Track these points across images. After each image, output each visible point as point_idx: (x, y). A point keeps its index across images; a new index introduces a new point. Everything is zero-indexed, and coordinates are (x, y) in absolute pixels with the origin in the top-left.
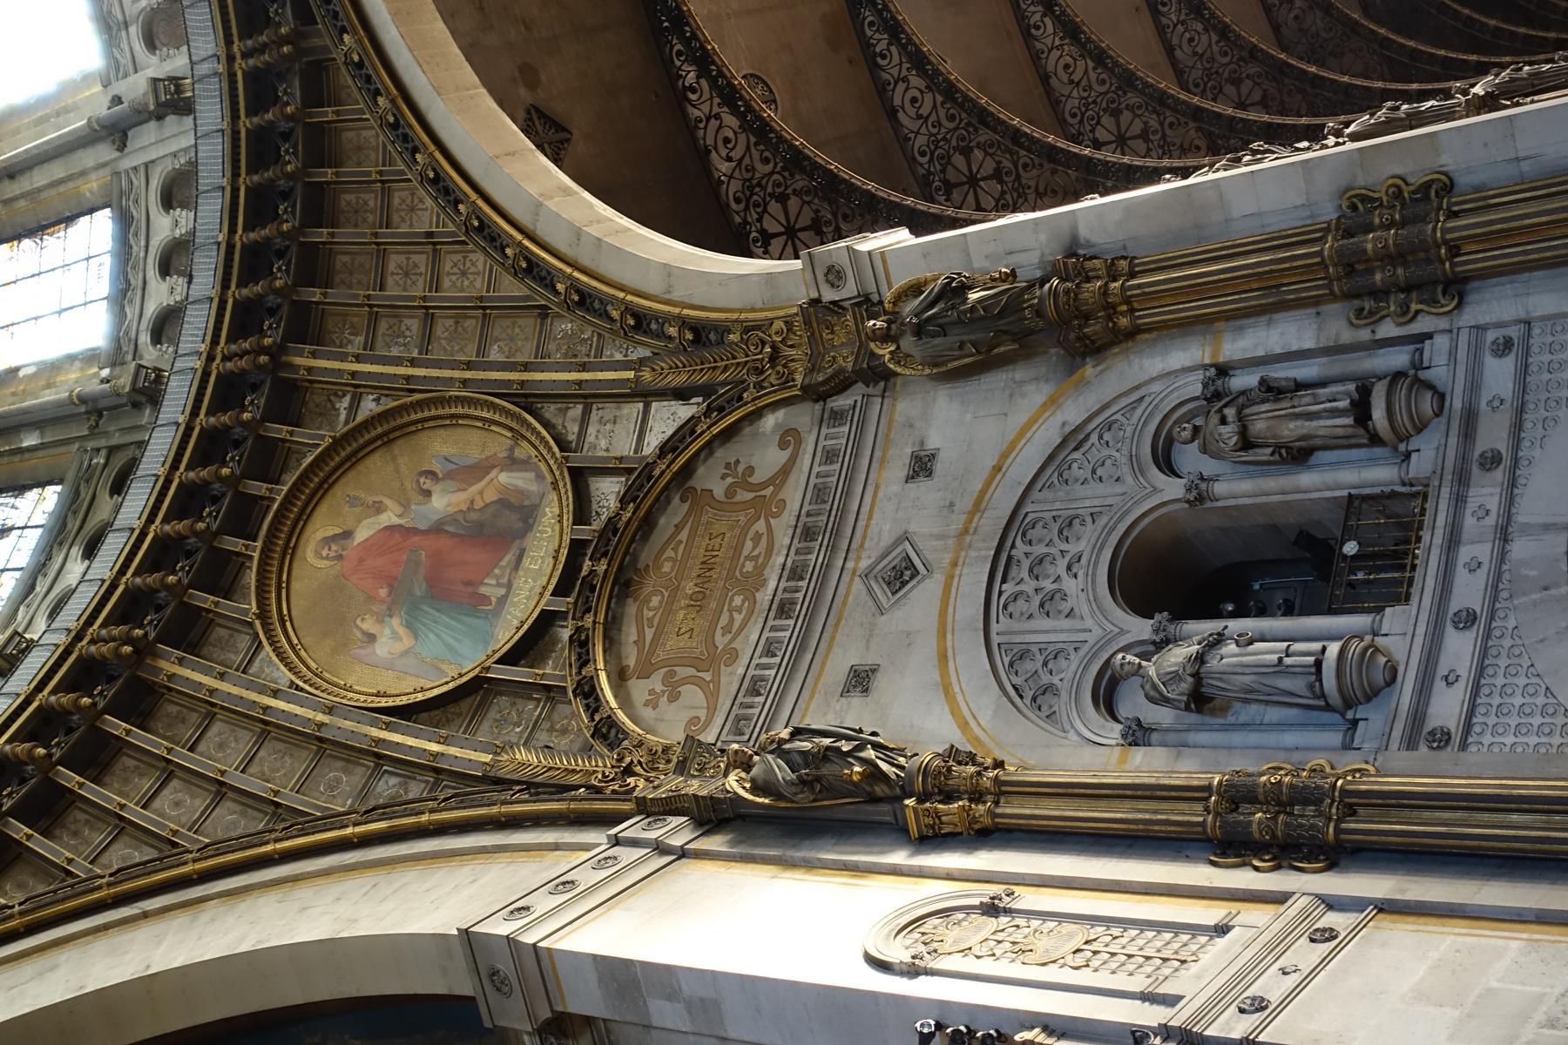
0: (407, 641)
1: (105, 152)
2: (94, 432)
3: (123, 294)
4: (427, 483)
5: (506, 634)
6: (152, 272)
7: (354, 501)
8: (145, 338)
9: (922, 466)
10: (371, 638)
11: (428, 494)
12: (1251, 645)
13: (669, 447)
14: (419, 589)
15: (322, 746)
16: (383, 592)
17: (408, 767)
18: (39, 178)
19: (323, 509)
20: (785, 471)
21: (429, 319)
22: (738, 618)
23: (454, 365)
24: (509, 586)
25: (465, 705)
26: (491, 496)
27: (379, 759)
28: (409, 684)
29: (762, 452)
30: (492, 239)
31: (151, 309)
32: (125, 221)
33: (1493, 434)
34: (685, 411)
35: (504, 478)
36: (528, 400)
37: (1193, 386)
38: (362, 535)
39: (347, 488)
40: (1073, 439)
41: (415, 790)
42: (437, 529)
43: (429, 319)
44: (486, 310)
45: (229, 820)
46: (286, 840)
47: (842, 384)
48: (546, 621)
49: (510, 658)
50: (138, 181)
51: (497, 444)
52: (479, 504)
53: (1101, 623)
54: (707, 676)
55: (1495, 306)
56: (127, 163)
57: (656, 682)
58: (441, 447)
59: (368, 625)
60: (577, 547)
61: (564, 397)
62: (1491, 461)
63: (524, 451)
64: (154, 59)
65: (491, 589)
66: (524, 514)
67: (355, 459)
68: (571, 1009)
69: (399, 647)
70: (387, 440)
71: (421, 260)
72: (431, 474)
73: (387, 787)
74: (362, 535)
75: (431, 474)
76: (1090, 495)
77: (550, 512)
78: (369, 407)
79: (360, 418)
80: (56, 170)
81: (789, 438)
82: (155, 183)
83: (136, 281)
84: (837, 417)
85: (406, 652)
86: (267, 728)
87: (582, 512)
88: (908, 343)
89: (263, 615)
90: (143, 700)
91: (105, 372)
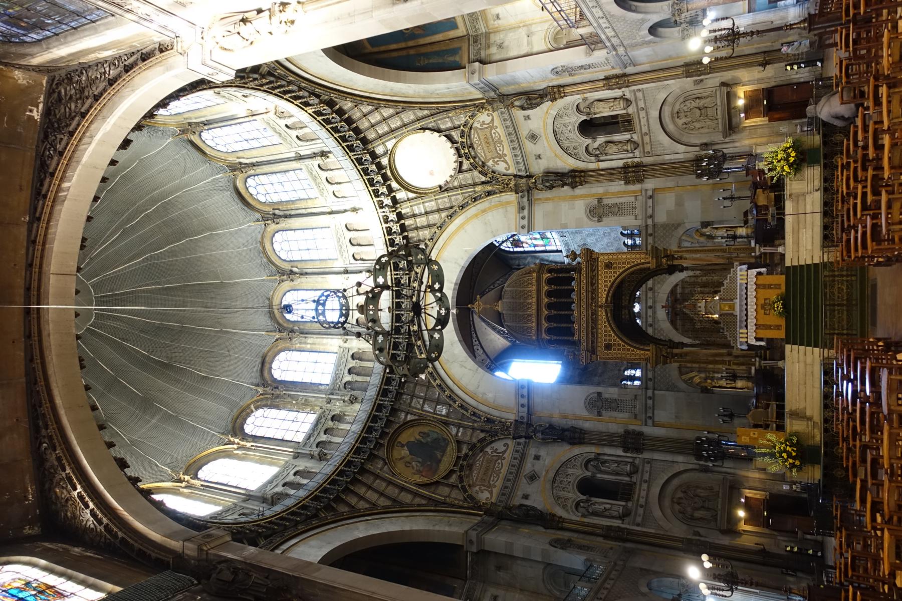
9: (537, 458)
12: (601, 504)
13: (480, 441)
15: (402, 489)
17: (422, 496)
20: (505, 451)
27: (416, 494)
29: (499, 446)
33: (646, 477)
34: (482, 435)
37: (593, 456)
40: (569, 460)
41: (424, 502)
45: (383, 502)
46: (397, 508)
47: (520, 437)
48: (452, 472)
53: (575, 495)
55: (647, 455)
57: (477, 488)
60: (458, 458)
62: (646, 481)
68: (486, 549)
71: (425, 389)
73: (418, 500)
76: (570, 471)
78: (409, 417)
81: (506, 445)
84: (519, 444)
86: (390, 483)
88: (539, 435)
90: (363, 471)
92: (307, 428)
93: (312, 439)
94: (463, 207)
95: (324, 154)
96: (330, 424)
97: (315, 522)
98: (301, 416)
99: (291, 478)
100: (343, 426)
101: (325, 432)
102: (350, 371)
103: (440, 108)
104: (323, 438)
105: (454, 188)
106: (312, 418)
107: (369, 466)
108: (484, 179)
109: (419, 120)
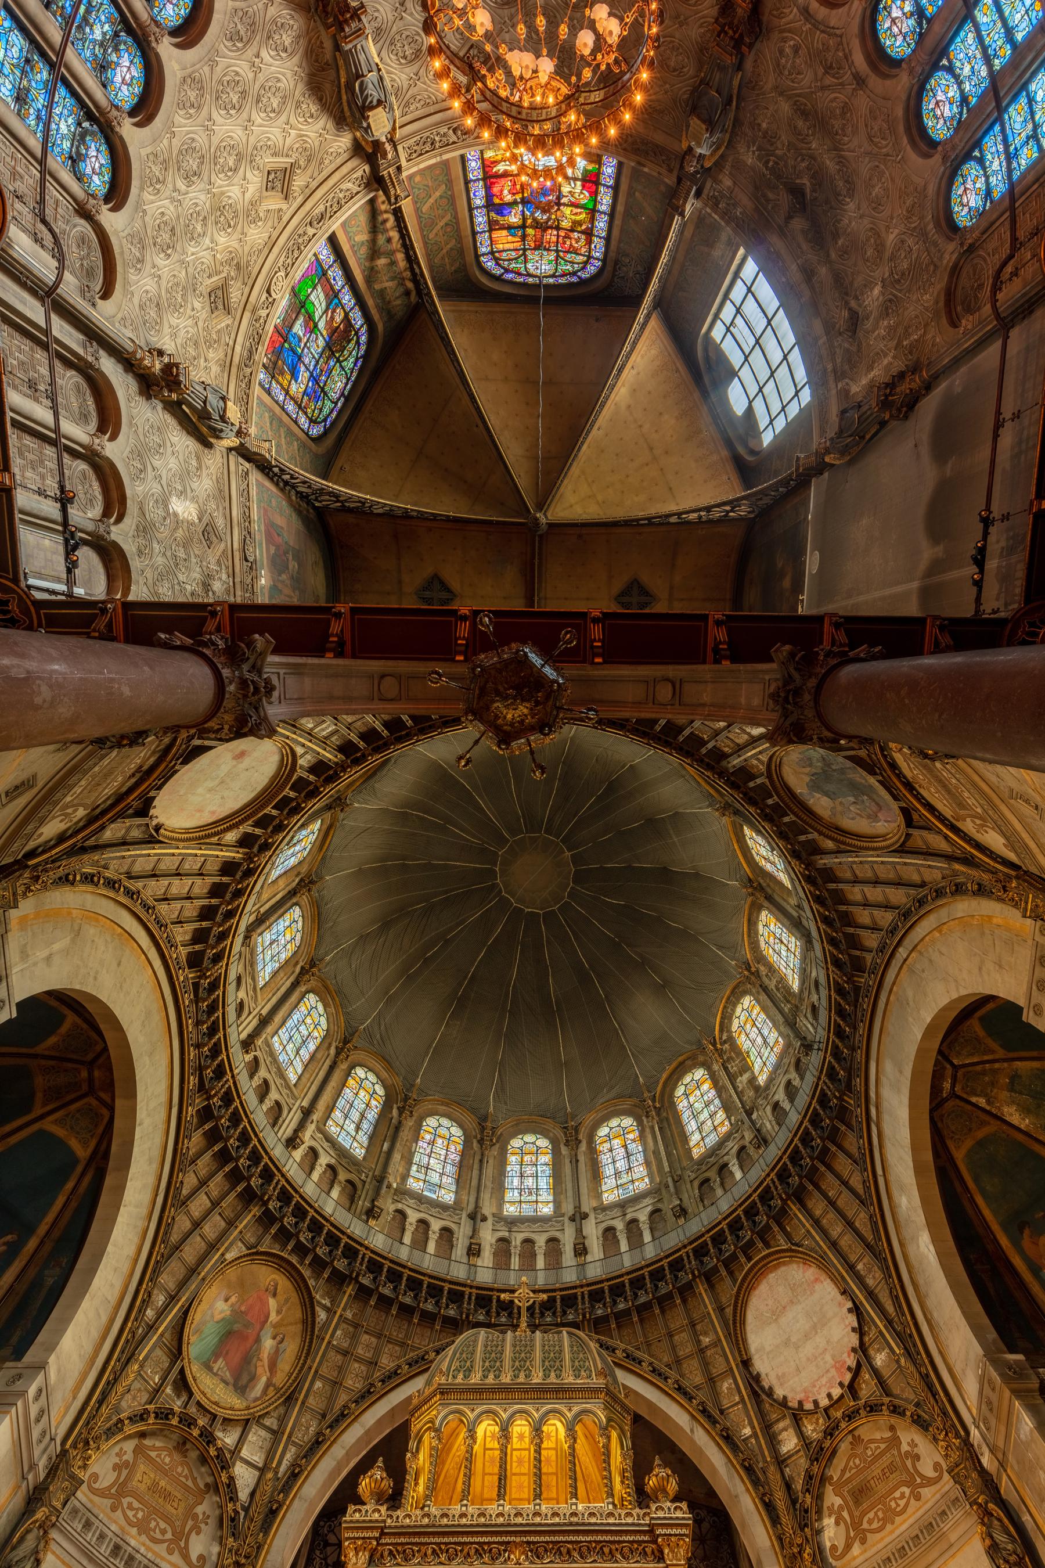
0: (218, 1317)
1: (471, 1207)
2: (374, 1176)
3: (420, 1199)
4: (278, 1338)
5: (195, 1371)
6: (422, 1215)
7: (287, 1301)
8: (400, 1206)
10: (226, 1300)
11: (274, 1338)
14: (237, 1327)
16: (243, 1308)
18: (475, 1172)
19: (290, 1286)
21: (345, 1353)
22: (130, 1514)
23: (320, 1364)
24: (216, 1374)
25: (175, 1343)
26: (260, 1370)
28: (198, 1317)
30: (363, 1397)
31: (409, 1212)
32: (444, 1207)
35: (264, 1379)
36: (289, 1400)
38: (272, 1303)
39: (295, 1298)
42: (258, 1340)
43: (345, 1353)
44: (336, 1384)
49: (182, 1371)
50: (456, 1219)
51: (280, 1379)
52: (259, 1364)
54: (113, 1491)
56: (464, 1215)
58: (291, 1348)
59: (233, 1299)
61: (282, 1420)
63: (271, 1392)
64: (494, 1241)
65: (219, 1364)
66: (241, 1389)
67: (303, 1304)
69: (216, 1313)
70: (304, 1322)
72: (281, 1342)
74: (272, 1303)
75: (281, 1342)
77: (237, 1402)
79: (317, 1308)
80: (474, 1182)
82: (453, 1226)
83: (422, 1207)
85: (212, 1316)
87: (227, 1421)
89: (257, 1253)
91: (395, 1185)
92: (345, 1141)
93: (326, 1145)
94: (728, 1438)
95: (762, 1140)
96: (342, 1176)
97: (193, 1081)
98: (364, 1139)
99: (274, 1095)
100: (335, 1193)
101: (330, 1166)
102: (423, 1223)
103: (912, 1343)
104: (324, 1160)
105: (762, 1414)
106: (359, 1152)
107: (256, 1211)
108: (798, 1485)
109: (871, 1295)
